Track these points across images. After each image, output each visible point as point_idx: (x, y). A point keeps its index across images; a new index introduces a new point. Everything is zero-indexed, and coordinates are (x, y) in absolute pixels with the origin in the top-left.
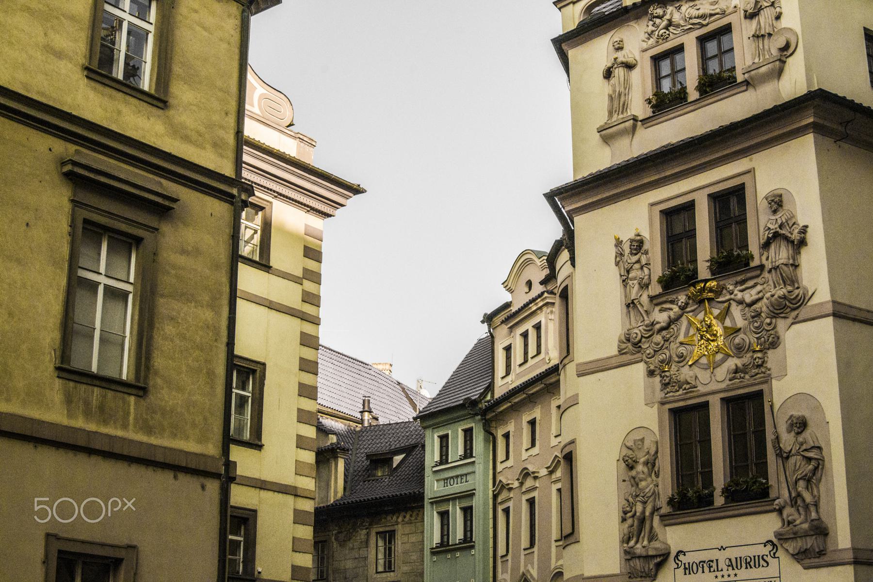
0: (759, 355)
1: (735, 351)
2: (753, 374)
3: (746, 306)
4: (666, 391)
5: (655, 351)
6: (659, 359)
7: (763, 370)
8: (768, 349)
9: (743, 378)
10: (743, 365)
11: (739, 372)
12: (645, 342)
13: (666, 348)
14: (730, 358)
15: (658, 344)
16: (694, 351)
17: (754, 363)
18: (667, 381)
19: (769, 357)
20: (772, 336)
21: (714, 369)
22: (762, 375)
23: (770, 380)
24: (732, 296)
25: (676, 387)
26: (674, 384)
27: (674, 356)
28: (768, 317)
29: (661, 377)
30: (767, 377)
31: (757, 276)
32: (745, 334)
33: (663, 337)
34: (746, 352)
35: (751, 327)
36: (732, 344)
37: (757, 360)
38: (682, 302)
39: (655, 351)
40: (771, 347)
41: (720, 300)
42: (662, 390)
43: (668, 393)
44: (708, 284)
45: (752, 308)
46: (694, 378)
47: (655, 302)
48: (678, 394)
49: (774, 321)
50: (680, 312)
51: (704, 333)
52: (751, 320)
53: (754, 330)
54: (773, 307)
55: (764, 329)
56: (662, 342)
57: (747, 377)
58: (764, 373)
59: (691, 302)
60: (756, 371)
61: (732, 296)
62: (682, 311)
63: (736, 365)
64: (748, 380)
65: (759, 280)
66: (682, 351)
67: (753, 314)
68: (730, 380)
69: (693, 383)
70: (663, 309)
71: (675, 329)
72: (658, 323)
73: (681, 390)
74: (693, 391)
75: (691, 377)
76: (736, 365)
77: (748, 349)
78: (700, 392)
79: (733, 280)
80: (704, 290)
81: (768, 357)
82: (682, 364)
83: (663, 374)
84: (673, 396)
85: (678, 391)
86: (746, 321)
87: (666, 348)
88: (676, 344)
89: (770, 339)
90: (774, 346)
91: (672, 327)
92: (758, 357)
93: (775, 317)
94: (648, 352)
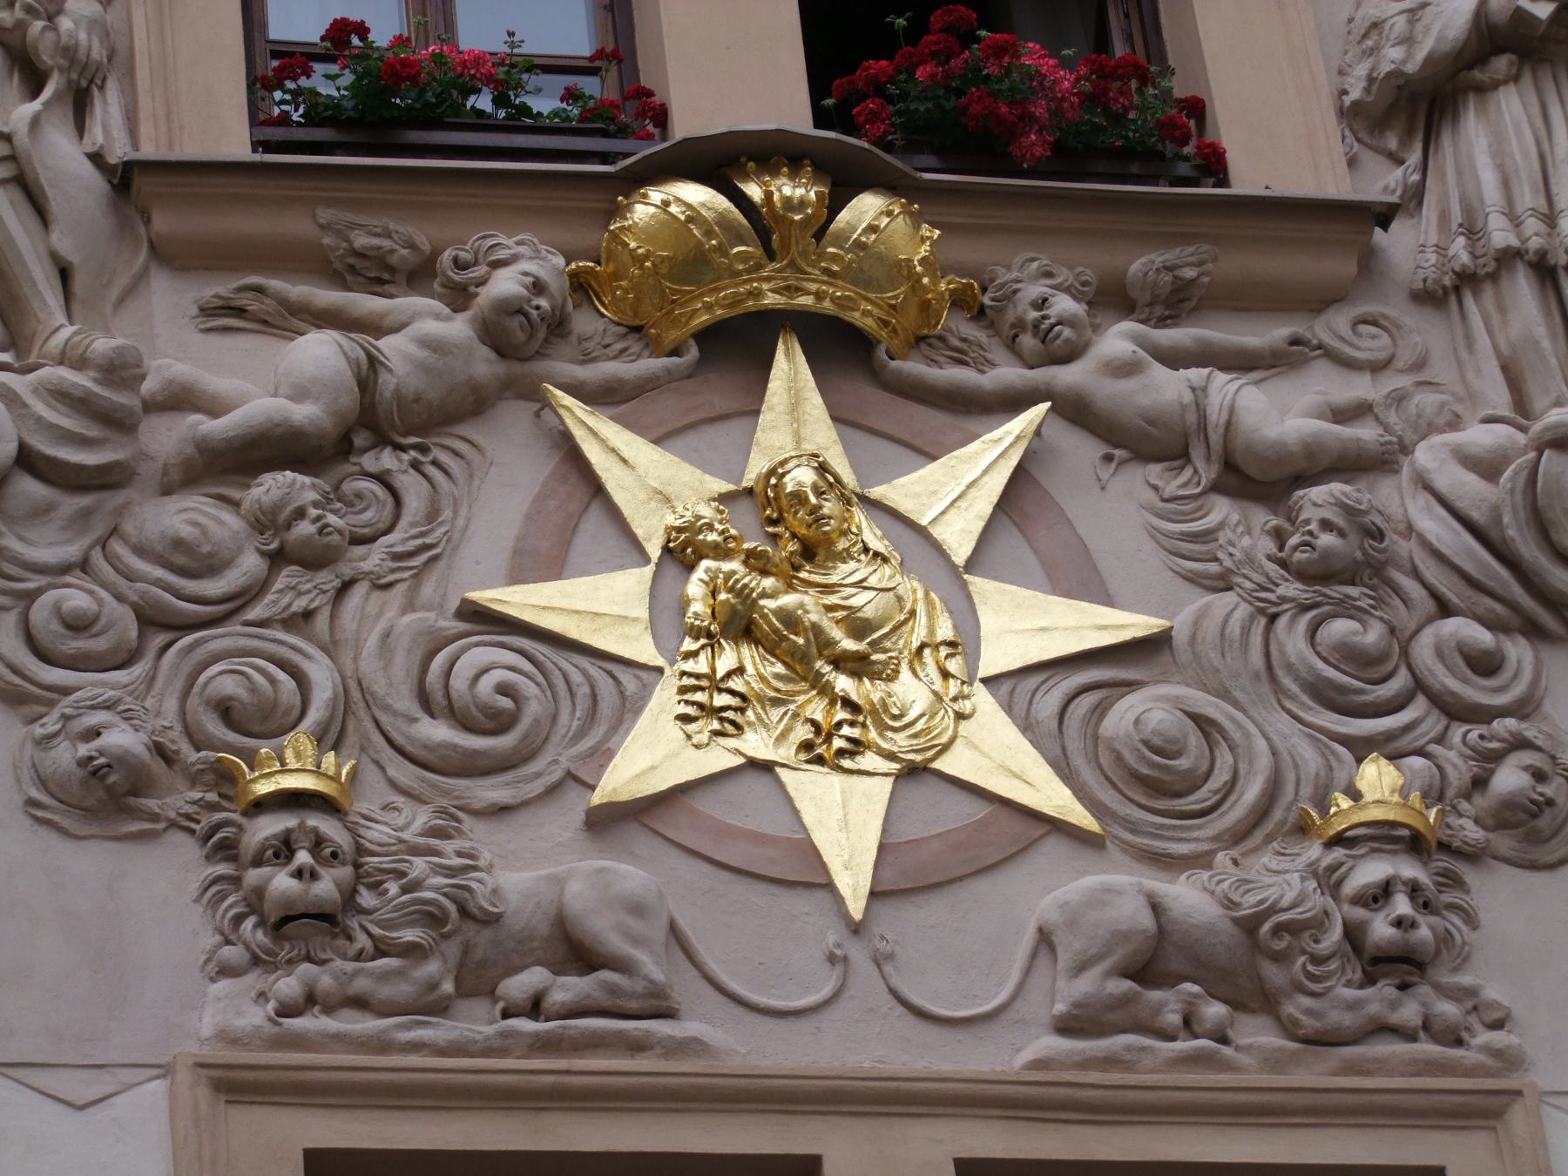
0: (1409, 869)
1: (1108, 797)
2: (1347, 1020)
3: (1216, 488)
4: (288, 985)
5: (151, 619)
6: (229, 686)
7: (1448, 1009)
8: (1473, 856)
9: (1224, 1040)
10: (1249, 926)
11: (1169, 980)
12: (40, 513)
13: (301, 621)
14: (1054, 847)
15: (211, 566)
16: (630, 708)
17: (1354, 934)
18: (326, 887)
19: (1484, 917)
20: (1528, 757)
21: (874, 895)
22: (1427, 1048)
23: (1517, 1116)
24: (1067, 376)
25: (432, 967)
26: (410, 935)
27: (408, 704)
28: (1445, 609)
29: (226, 850)
30: (1470, 1072)
31: (1319, 301)
32: (1225, 695)
33: (265, 522)
34: (1238, 836)
35: (1292, 640)
36: (1075, 745)
37: (1402, 905)
38: (538, 287)
39: (151, 619)
40: (1504, 843)
41: (914, 367)
42: (226, 971)
43: (311, 1000)
44: (866, 208)
45: (1317, 493)
46: (659, 932)
47: (164, 222)
48: (439, 1031)
49: (1518, 651)
50: (484, 365)
51: (768, 583)
52: (1292, 589)
53: (1330, 673)
54: (1541, 525)
55: (1420, 685)
56: (250, 564)
57: (1257, 1034)
58: (1459, 1042)
59: (584, 323)
60: (1378, 998)
61: (1067, 376)
62: (501, 368)
63: (1156, 907)
64: (1274, 1061)
65: (1333, 326)
66: (487, 684)
67: (1326, 540)
68: (1065, 1027)
69: (652, 967)
70: (244, 300)
71: (409, 483)
72: (180, 400)
73: (479, 1007)
74: (637, 1046)
75: (637, 909)
76: (1156, 907)
77: (1261, 813)
78: (732, 1064)
79: (1094, 261)
80: (820, 235)
81: (1471, 920)
82: (490, 791)
83: (269, 826)
84: (382, 1045)
85: (440, 1009)
86: (1229, 598)
87: (301, 621)
88: (409, 606)
89: (1509, 779)
90: (1536, 838)
91: (369, 462)
92: (1414, 889)
93: (1533, 631)
94: (76, 599)
